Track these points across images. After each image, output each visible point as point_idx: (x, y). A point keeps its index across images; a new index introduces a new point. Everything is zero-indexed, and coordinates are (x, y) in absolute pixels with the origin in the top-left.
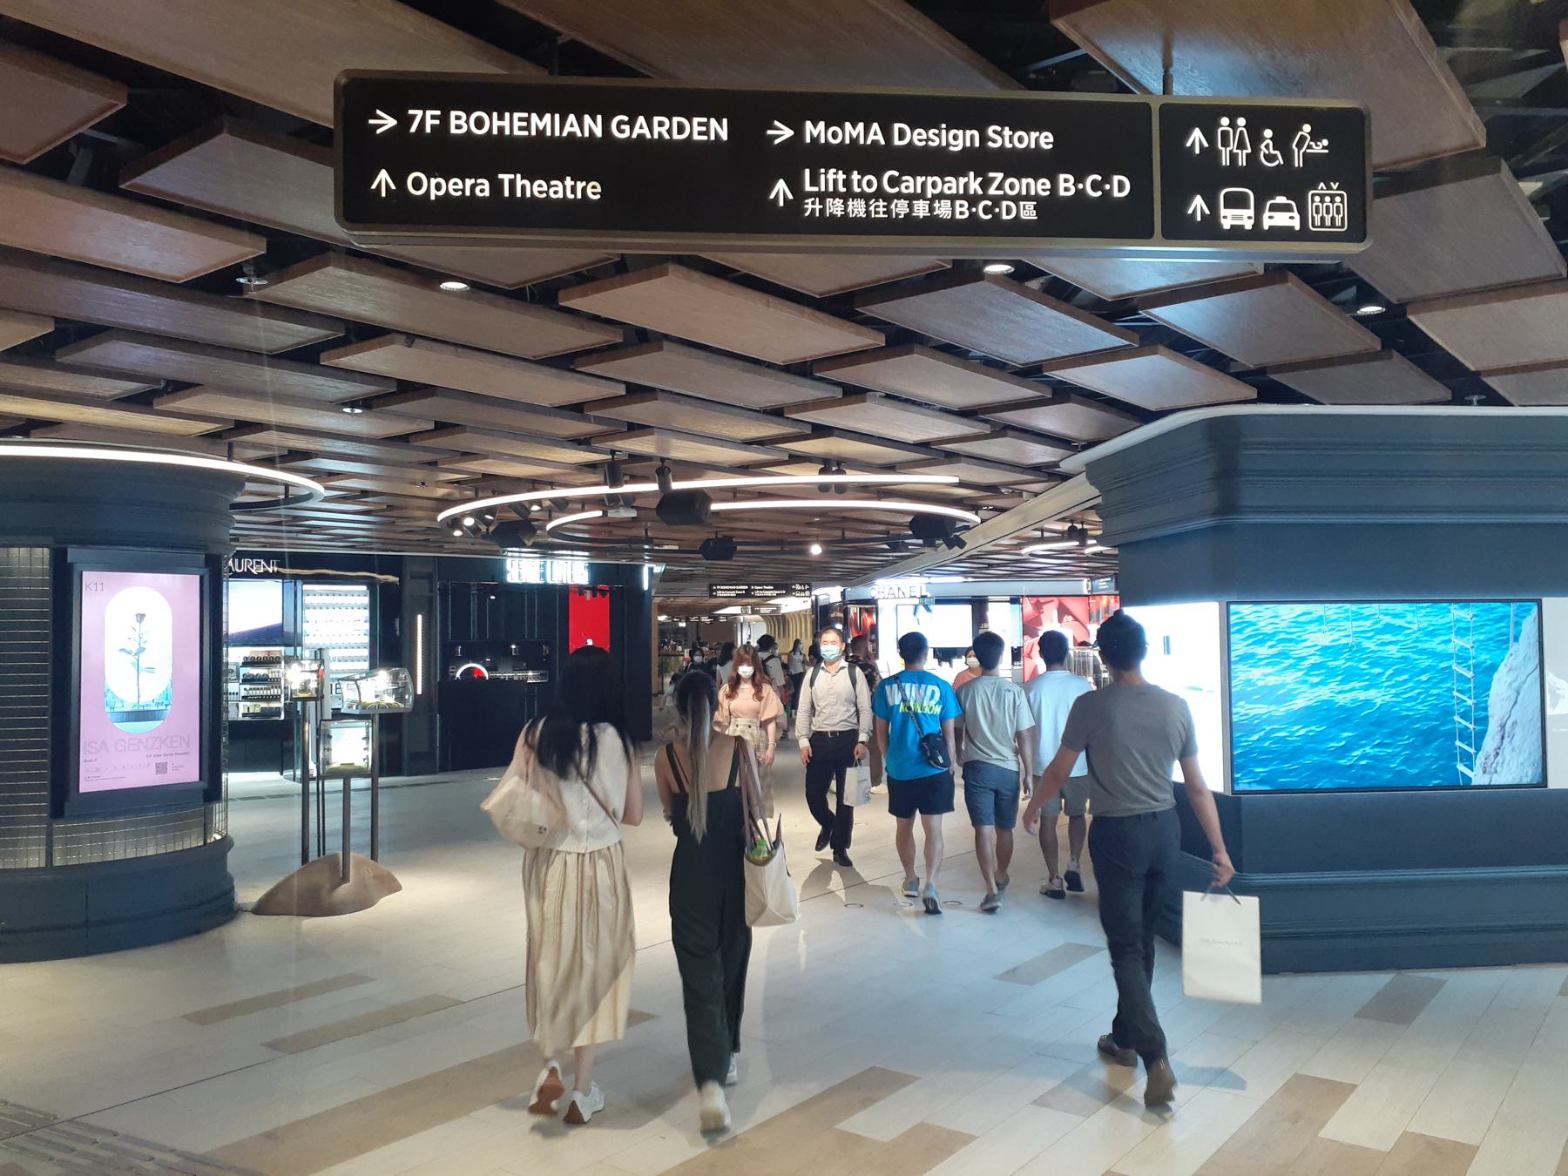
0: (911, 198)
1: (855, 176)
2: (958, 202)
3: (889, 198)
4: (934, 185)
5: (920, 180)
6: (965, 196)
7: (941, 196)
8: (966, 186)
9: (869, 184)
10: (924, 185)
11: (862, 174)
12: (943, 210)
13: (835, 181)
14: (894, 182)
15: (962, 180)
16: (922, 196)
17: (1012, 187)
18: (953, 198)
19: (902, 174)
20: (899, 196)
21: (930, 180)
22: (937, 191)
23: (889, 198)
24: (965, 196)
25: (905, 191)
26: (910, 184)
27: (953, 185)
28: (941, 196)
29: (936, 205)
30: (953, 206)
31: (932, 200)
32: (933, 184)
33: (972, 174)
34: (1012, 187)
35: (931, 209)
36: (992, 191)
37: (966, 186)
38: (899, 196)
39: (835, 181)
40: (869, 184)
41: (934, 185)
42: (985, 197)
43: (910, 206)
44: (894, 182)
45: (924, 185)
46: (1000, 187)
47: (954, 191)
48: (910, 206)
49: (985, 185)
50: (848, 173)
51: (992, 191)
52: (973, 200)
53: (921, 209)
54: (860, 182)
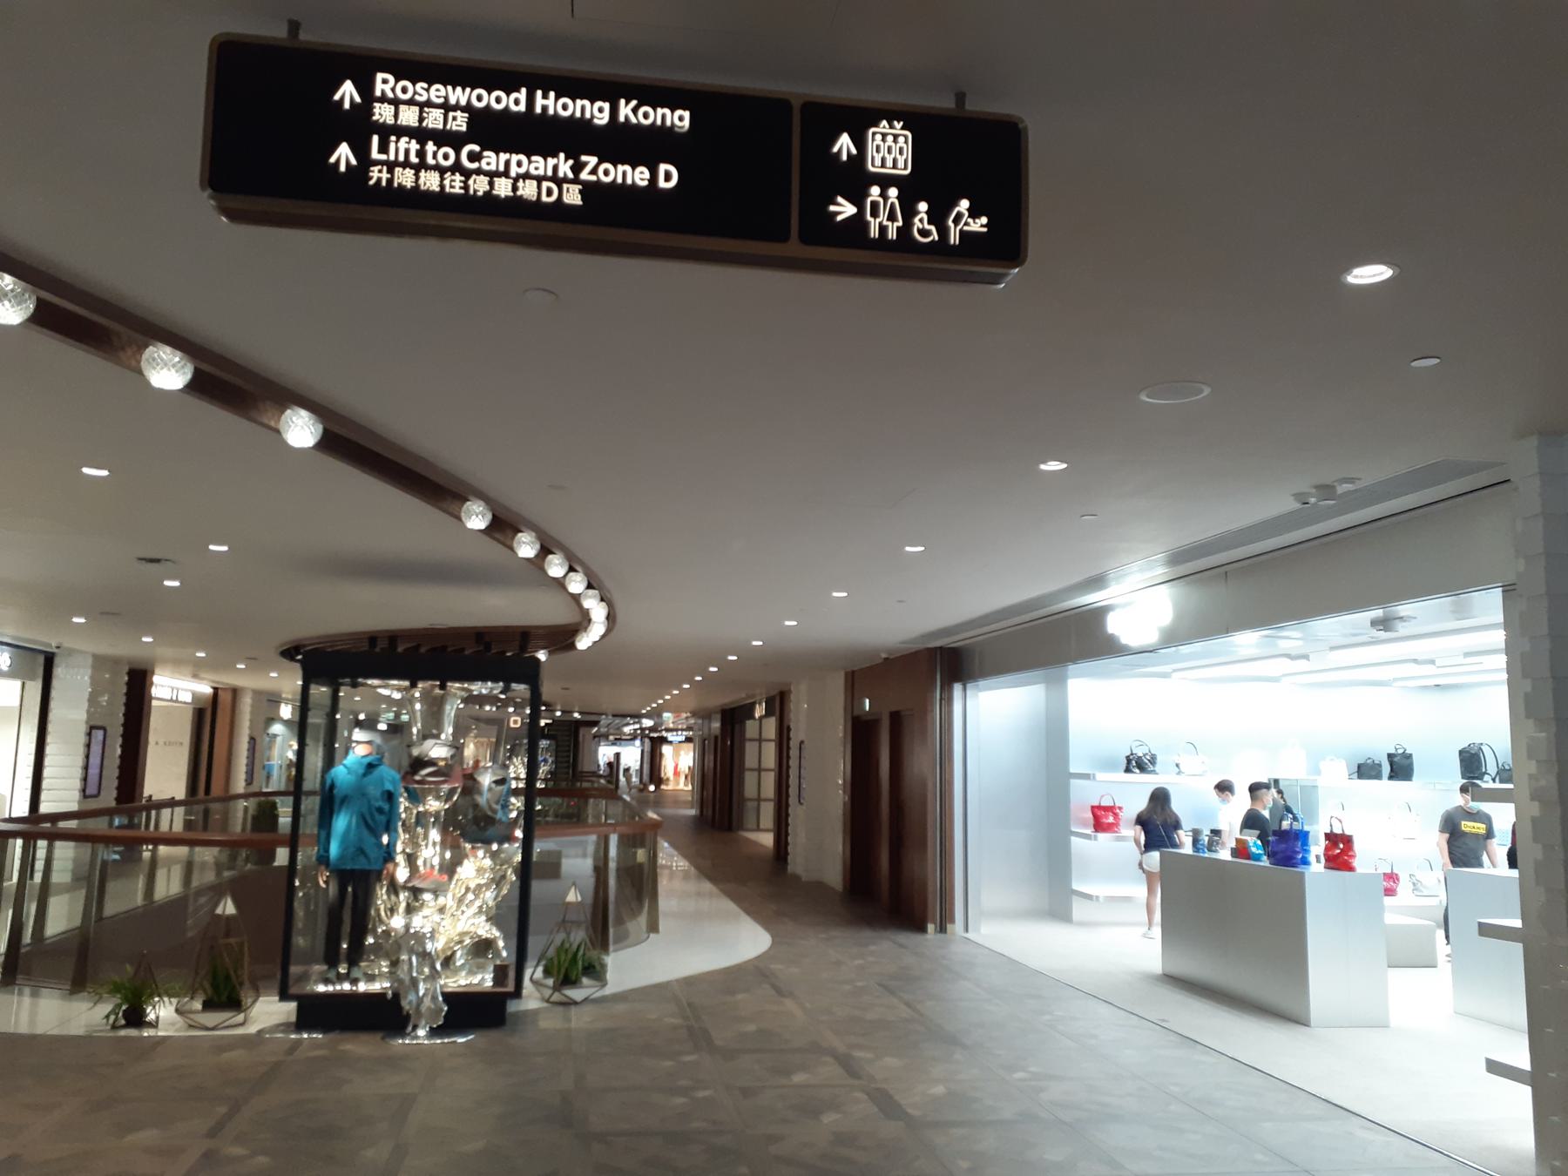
0: (492, 175)
1: (430, 147)
2: (545, 184)
3: (467, 174)
4: (519, 164)
5: (504, 157)
7: (526, 176)
8: (555, 168)
9: (446, 157)
10: (507, 163)
11: (439, 145)
12: (528, 190)
13: (407, 152)
15: (551, 161)
16: (506, 174)
17: (606, 173)
19: (483, 149)
20: (479, 172)
21: (515, 158)
22: (522, 170)
23: (467, 174)
24: (555, 178)
25: (485, 167)
26: (491, 160)
27: (539, 165)
28: (526, 176)
29: (520, 184)
30: (539, 187)
31: (516, 180)
32: (518, 162)
33: (562, 156)
34: (606, 173)
35: (515, 188)
36: (584, 176)
37: (555, 168)
38: (479, 172)
39: (407, 152)
40: (446, 157)
41: (519, 164)
42: (576, 181)
43: (491, 184)
44: (473, 157)
45: (507, 163)
46: (594, 172)
47: (541, 172)
48: (491, 184)
49: (577, 168)
51: (584, 176)
52: (559, 182)
54: (435, 155)
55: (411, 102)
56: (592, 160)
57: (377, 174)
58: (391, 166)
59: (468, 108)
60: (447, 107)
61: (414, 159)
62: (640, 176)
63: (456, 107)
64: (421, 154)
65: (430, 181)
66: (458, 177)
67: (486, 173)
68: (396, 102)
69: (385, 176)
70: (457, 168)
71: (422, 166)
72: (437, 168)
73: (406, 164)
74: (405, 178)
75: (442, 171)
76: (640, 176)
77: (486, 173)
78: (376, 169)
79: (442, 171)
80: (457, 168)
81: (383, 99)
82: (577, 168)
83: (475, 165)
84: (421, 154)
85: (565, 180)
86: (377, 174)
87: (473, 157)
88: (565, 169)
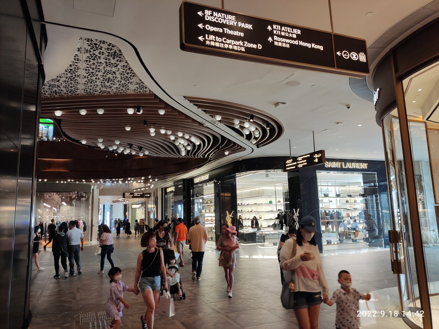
5: (230, 41)
6: (240, 46)
7: (235, 45)
11: (219, 37)
12: (235, 48)
14: (225, 40)
15: (239, 42)
16: (231, 44)
18: (237, 46)
20: (226, 43)
21: (232, 41)
23: (224, 43)
26: (228, 41)
27: (237, 43)
28: (235, 45)
32: (233, 42)
36: (245, 45)
38: (226, 43)
46: (247, 45)
49: (244, 44)
50: (215, 36)
51: (245, 45)
53: (231, 47)
55: (280, 42)
56: (246, 43)
57: (208, 42)
58: (210, 41)
59: (289, 43)
60: (286, 43)
61: (214, 40)
62: (255, 46)
63: (287, 43)
64: (215, 39)
65: (217, 45)
66: (222, 44)
67: (228, 44)
68: (278, 41)
69: (209, 43)
70: (222, 42)
71: (215, 41)
72: (218, 42)
73: (213, 41)
74: (213, 44)
75: (220, 42)
76: (255, 46)
77: (228, 44)
78: (207, 41)
79: (220, 42)
80: (222, 42)
81: (276, 41)
82: (244, 44)
83: (225, 42)
84: (215, 39)
85: (242, 46)
86: (208, 42)
87: (225, 40)
88: (242, 44)
